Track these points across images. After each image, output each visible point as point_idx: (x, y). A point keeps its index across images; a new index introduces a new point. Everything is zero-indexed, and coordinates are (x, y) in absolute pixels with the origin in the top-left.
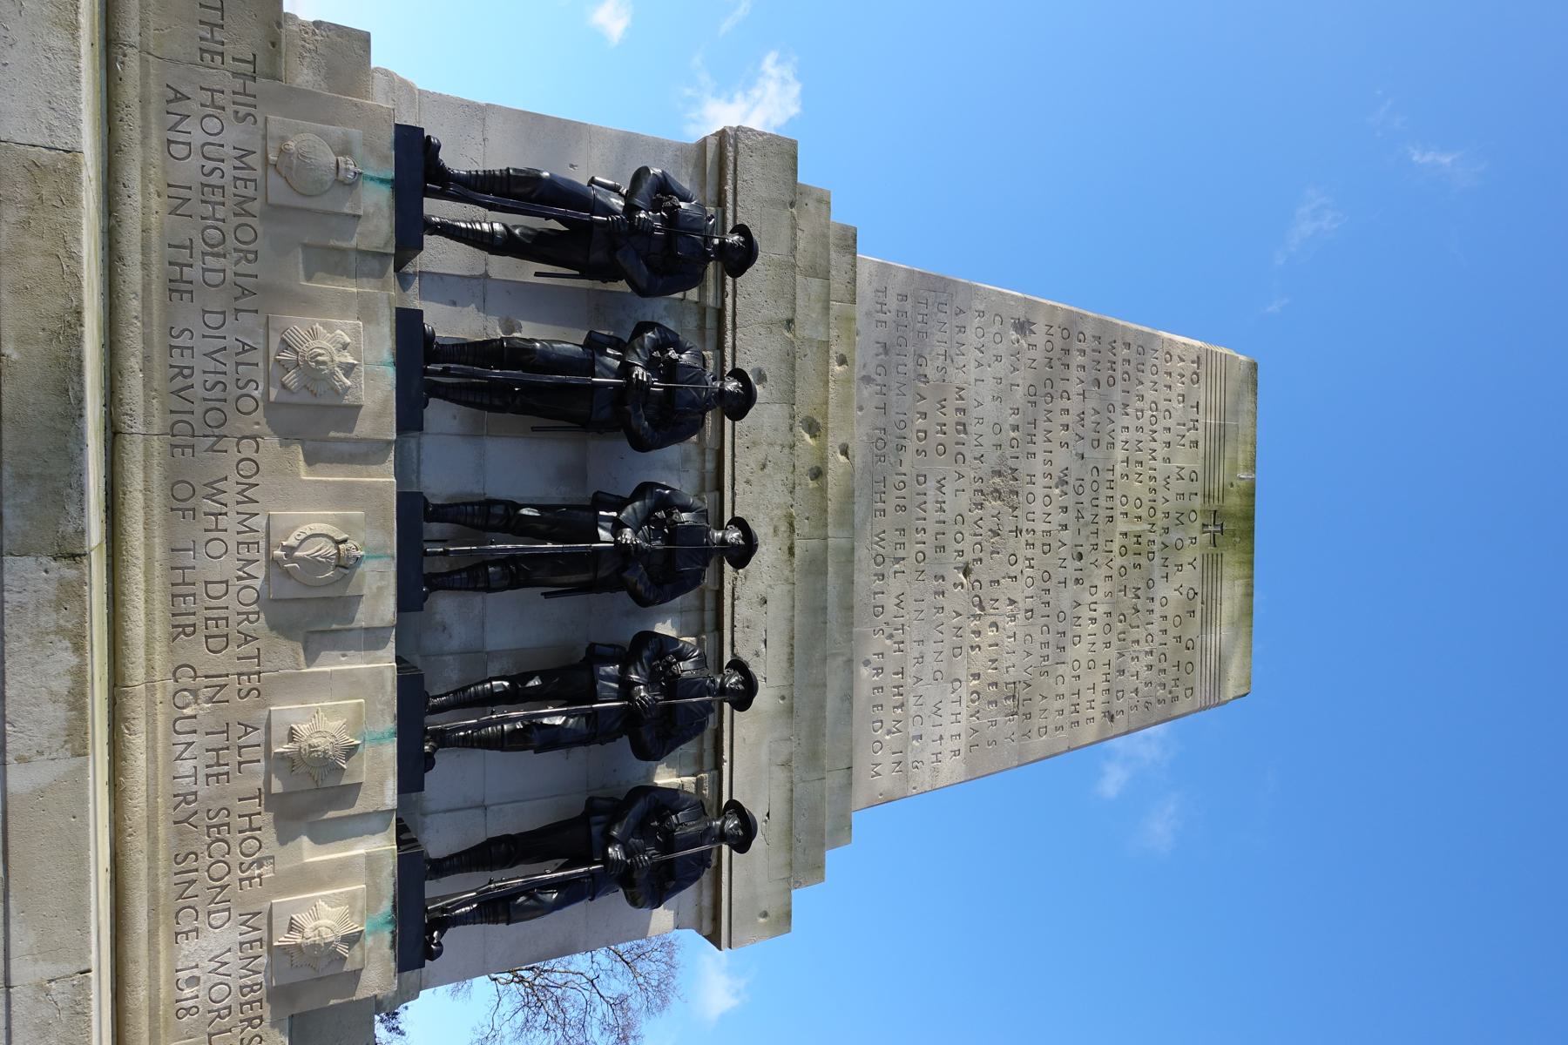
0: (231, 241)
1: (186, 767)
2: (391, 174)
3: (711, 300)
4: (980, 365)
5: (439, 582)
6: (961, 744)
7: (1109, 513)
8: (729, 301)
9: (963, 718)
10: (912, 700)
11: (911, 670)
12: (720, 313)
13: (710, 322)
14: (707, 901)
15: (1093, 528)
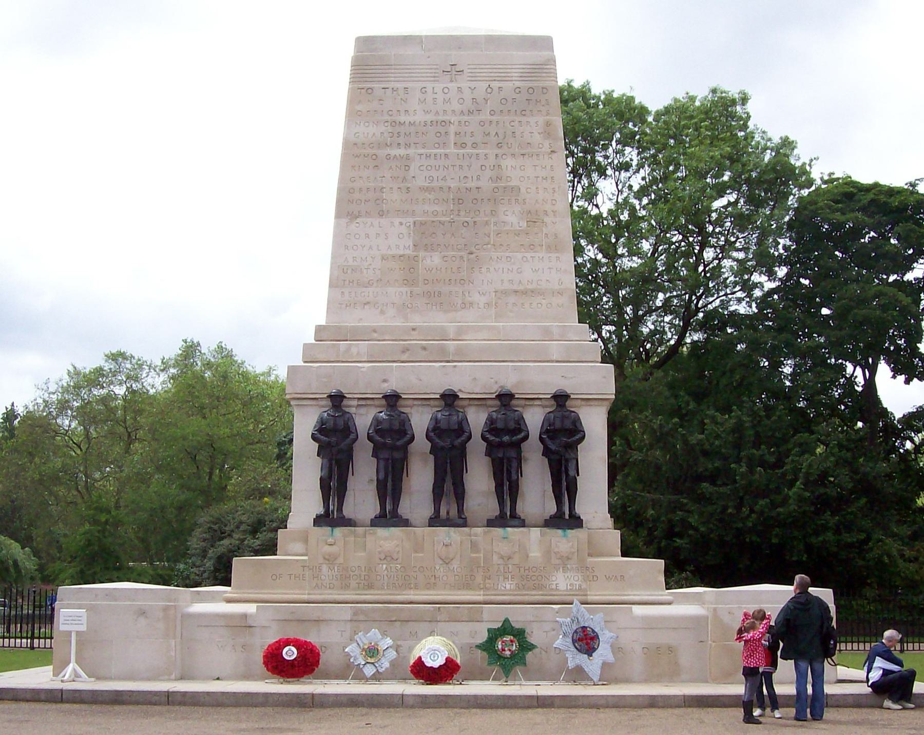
0: (356, 573)
1: (508, 587)
2: (330, 528)
3: (355, 403)
4: (371, 248)
5: (460, 510)
6: (554, 255)
7: (443, 157)
8: (356, 396)
9: (541, 255)
10: (530, 287)
11: (515, 287)
12: (359, 399)
13: (363, 402)
14: (596, 403)
15: (451, 168)
